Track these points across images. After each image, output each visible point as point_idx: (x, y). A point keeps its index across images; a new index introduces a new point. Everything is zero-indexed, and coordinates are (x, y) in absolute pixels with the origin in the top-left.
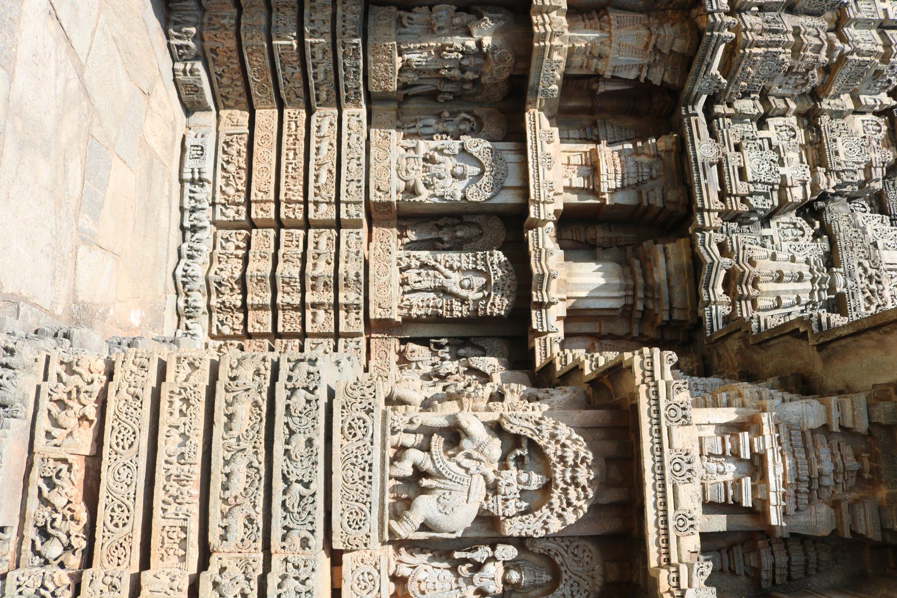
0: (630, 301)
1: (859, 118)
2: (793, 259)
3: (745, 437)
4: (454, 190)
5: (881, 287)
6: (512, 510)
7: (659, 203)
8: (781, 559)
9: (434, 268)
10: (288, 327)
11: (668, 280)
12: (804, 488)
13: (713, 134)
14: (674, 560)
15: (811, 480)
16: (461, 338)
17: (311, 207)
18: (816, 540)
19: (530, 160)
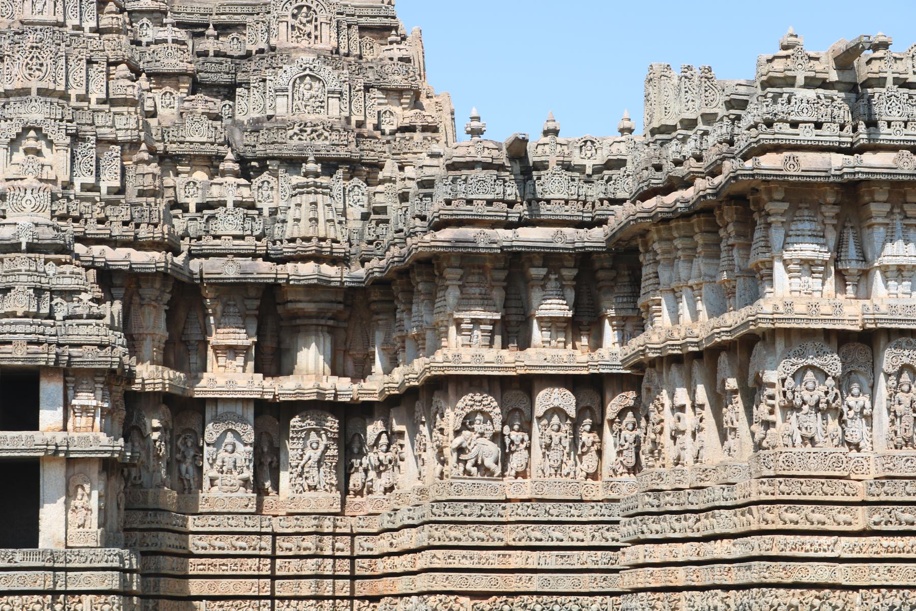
0: (326, 328)
1: (160, 111)
2: (299, 205)
3: (463, 326)
4: (244, 453)
5: (309, 124)
6: (491, 427)
7: (257, 303)
8: (513, 311)
9: (303, 468)
10: (346, 568)
11: (315, 302)
12: (486, 302)
13: (207, 256)
14: (513, 365)
15: (483, 299)
16: (346, 450)
17: (263, 553)
18: (507, 294)
19: (230, 396)
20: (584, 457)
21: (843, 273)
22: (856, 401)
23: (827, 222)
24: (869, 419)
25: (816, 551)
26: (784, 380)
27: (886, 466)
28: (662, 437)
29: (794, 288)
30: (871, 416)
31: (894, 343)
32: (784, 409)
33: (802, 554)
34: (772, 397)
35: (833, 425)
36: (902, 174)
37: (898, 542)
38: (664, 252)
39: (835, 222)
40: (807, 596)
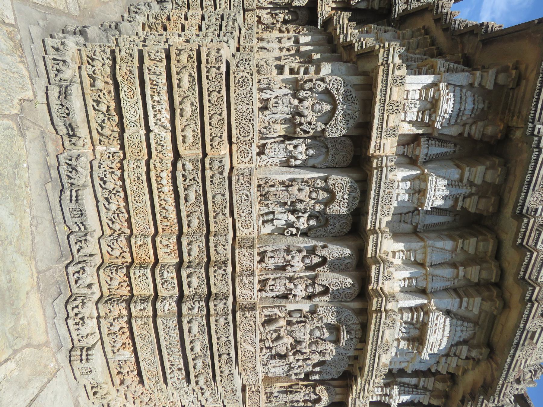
20: (269, 16)
21: (416, 143)
22: (301, 152)
23: (467, 128)
24: (286, 164)
25: (153, 108)
26: (323, 80)
27: (241, 177)
28: (277, 32)
29: (411, 93)
30: (289, 166)
31: (356, 185)
32: (296, 81)
33: (148, 93)
34: (306, 72)
35: (280, 130)
36: (526, 196)
37: (167, 188)
38: (404, 34)
39: (466, 135)
40: (107, 96)
